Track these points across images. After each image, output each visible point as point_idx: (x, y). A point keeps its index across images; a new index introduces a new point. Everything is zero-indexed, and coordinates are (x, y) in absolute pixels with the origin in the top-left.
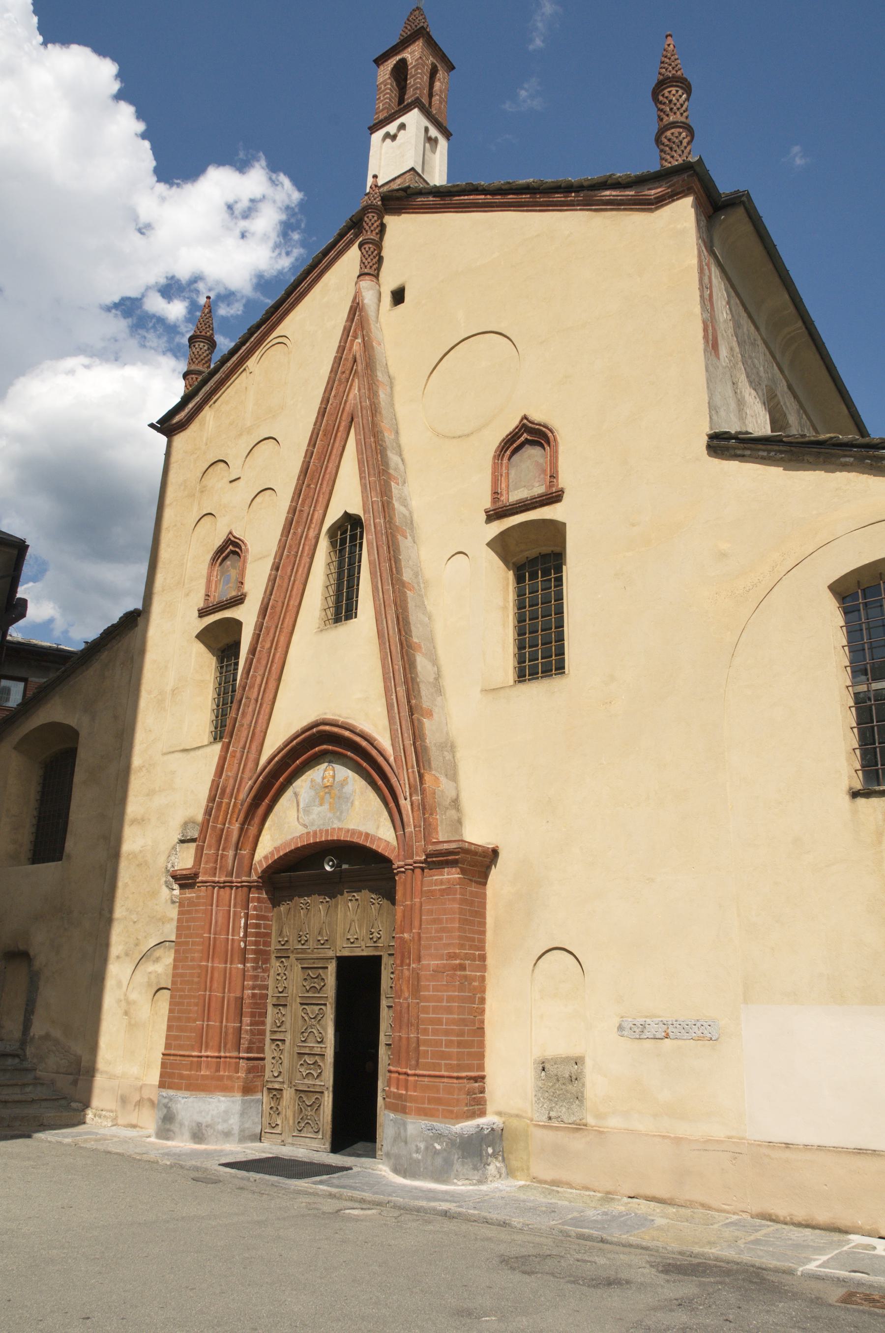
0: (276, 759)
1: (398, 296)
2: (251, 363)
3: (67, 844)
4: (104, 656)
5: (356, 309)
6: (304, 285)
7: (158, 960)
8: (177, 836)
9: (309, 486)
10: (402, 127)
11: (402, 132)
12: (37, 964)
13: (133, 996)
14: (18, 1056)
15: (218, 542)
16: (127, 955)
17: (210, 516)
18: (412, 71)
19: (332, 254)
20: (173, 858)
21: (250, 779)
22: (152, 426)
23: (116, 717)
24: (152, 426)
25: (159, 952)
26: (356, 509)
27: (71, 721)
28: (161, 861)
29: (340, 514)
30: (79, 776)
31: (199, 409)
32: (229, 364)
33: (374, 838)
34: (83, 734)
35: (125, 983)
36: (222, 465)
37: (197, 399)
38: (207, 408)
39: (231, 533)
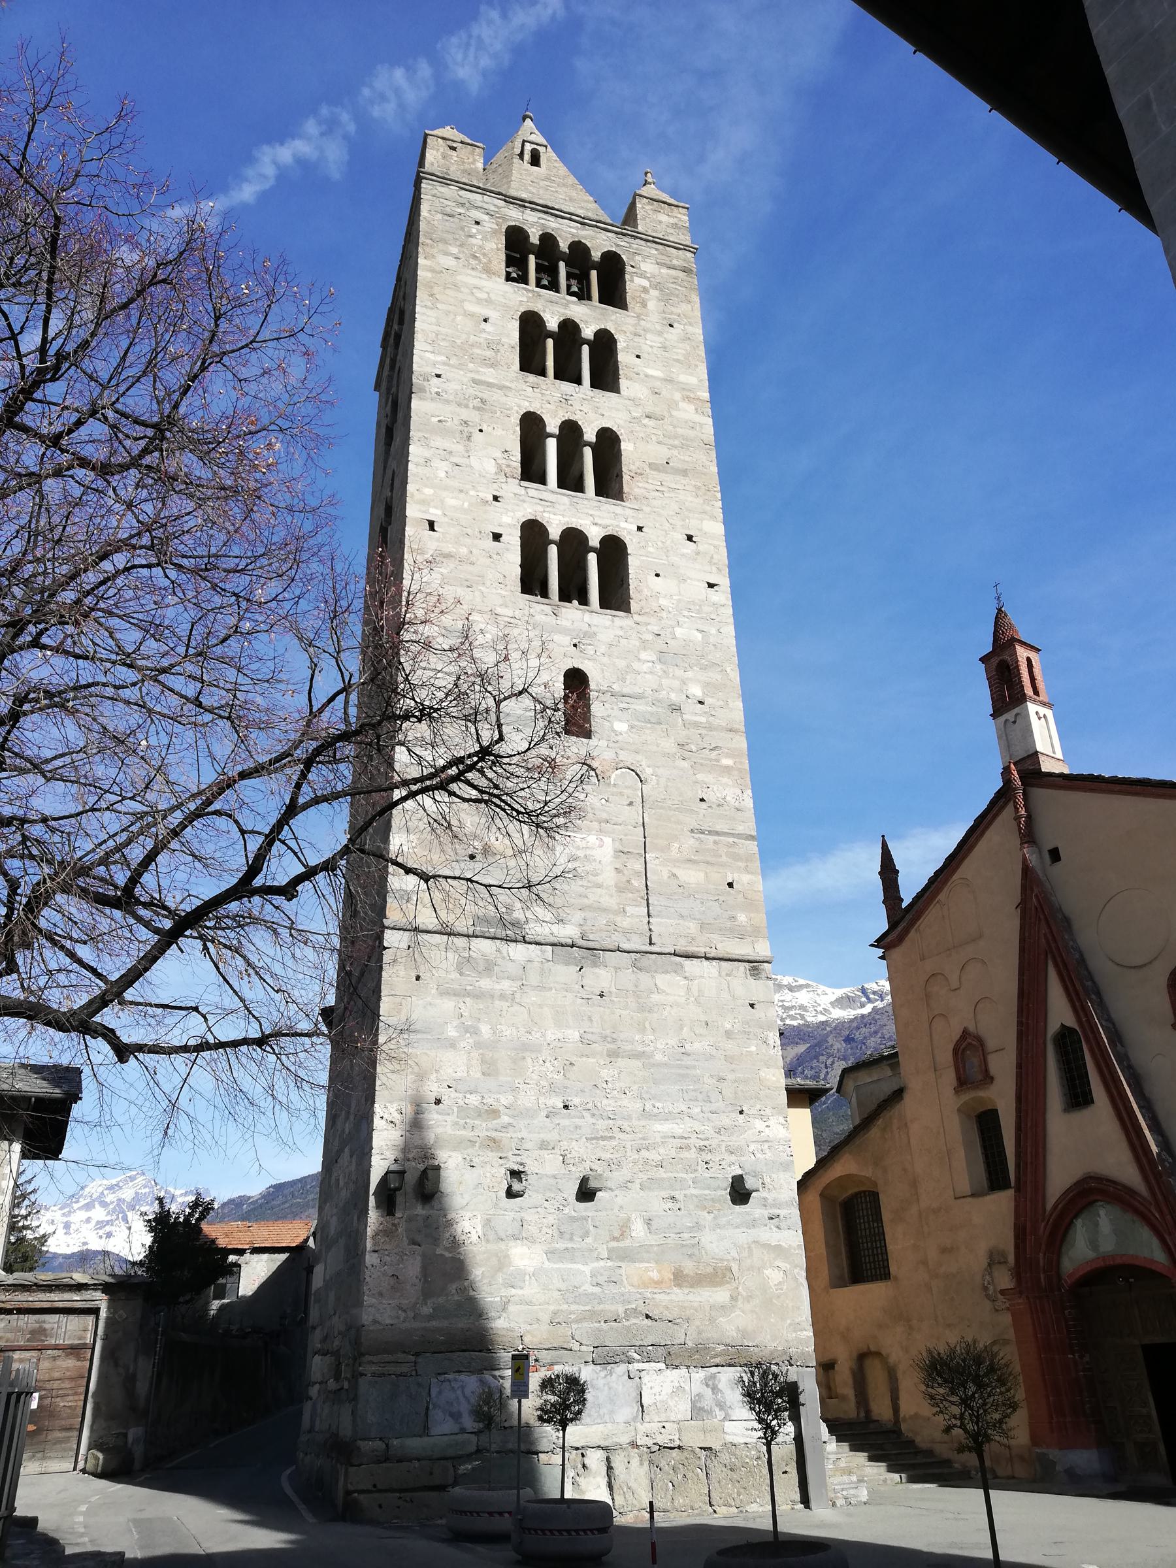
0: (1060, 1206)
1: (1055, 855)
2: (942, 896)
5: (1026, 870)
6: (972, 840)
8: (984, 1262)
9: (1028, 1005)
14: (894, 1432)
21: (1043, 1221)
22: (872, 945)
23: (905, 1170)
26: (1070, 1021)
27: (868, 1172)
29: (1059, 1026)
31: (906, 931)
33: (1152, 1261)
36: (939, 976)
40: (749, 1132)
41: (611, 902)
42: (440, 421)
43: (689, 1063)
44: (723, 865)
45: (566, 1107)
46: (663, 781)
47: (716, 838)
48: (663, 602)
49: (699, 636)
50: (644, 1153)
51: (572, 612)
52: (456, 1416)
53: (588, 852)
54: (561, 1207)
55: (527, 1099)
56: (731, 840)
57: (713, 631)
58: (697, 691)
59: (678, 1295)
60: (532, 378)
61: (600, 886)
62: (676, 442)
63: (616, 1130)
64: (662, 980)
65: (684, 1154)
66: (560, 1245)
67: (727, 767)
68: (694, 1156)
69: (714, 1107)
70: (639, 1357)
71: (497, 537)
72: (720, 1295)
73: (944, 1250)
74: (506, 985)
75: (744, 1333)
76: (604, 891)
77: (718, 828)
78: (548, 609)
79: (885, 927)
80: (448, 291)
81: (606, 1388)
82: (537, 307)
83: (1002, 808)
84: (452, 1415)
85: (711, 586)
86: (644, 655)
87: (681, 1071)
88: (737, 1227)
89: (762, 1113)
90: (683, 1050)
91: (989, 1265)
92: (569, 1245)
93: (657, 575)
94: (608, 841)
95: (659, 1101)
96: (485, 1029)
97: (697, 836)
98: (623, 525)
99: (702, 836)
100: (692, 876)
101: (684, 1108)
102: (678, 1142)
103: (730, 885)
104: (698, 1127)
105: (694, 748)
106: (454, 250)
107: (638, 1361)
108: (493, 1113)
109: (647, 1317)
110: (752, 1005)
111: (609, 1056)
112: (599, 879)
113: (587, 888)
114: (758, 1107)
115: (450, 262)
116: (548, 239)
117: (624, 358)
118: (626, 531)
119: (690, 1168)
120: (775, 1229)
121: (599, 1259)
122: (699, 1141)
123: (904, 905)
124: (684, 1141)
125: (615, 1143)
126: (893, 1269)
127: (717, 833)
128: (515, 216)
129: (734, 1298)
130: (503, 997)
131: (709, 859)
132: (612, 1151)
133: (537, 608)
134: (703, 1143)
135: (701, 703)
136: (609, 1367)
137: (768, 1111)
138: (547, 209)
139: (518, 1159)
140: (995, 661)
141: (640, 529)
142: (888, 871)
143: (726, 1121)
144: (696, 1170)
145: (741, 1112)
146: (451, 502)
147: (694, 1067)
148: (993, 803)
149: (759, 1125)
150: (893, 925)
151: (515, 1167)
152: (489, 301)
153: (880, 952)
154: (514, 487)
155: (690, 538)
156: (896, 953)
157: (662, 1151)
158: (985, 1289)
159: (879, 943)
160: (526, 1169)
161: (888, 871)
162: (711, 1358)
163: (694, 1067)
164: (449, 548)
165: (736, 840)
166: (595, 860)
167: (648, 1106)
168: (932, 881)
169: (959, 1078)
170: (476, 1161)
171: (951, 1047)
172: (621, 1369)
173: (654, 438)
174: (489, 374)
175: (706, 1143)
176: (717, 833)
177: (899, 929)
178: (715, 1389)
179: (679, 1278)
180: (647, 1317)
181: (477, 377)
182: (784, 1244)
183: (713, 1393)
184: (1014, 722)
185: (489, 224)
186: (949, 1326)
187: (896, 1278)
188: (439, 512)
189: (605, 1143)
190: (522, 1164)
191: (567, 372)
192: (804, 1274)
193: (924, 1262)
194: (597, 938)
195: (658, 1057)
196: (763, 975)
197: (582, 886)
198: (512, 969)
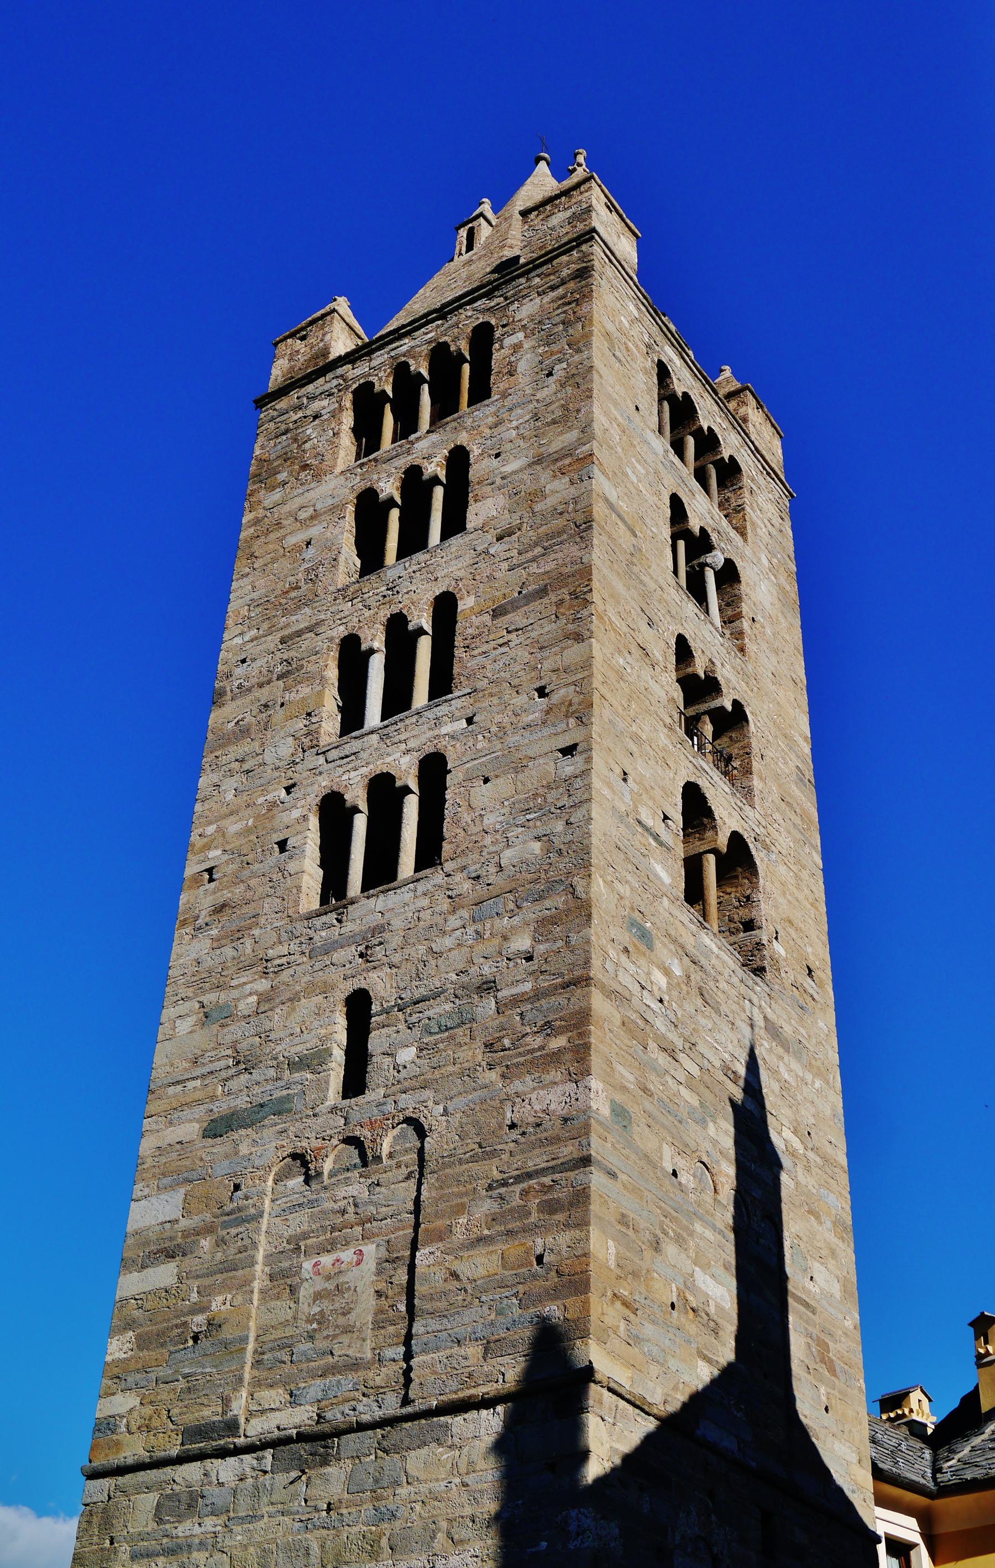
42: (237, 723)
53: (342, 1279)
56: (547, 1180)
57: (559, 826)
61: (348, 1330)
62: (538, 550)
64: (416, 1460)
74: (210, 1523)
77: (531, 1165)
93: (486, 781)
105: (507, 1042)
141: (470, 721)
188: (219, 852)
197: (327, 1337)
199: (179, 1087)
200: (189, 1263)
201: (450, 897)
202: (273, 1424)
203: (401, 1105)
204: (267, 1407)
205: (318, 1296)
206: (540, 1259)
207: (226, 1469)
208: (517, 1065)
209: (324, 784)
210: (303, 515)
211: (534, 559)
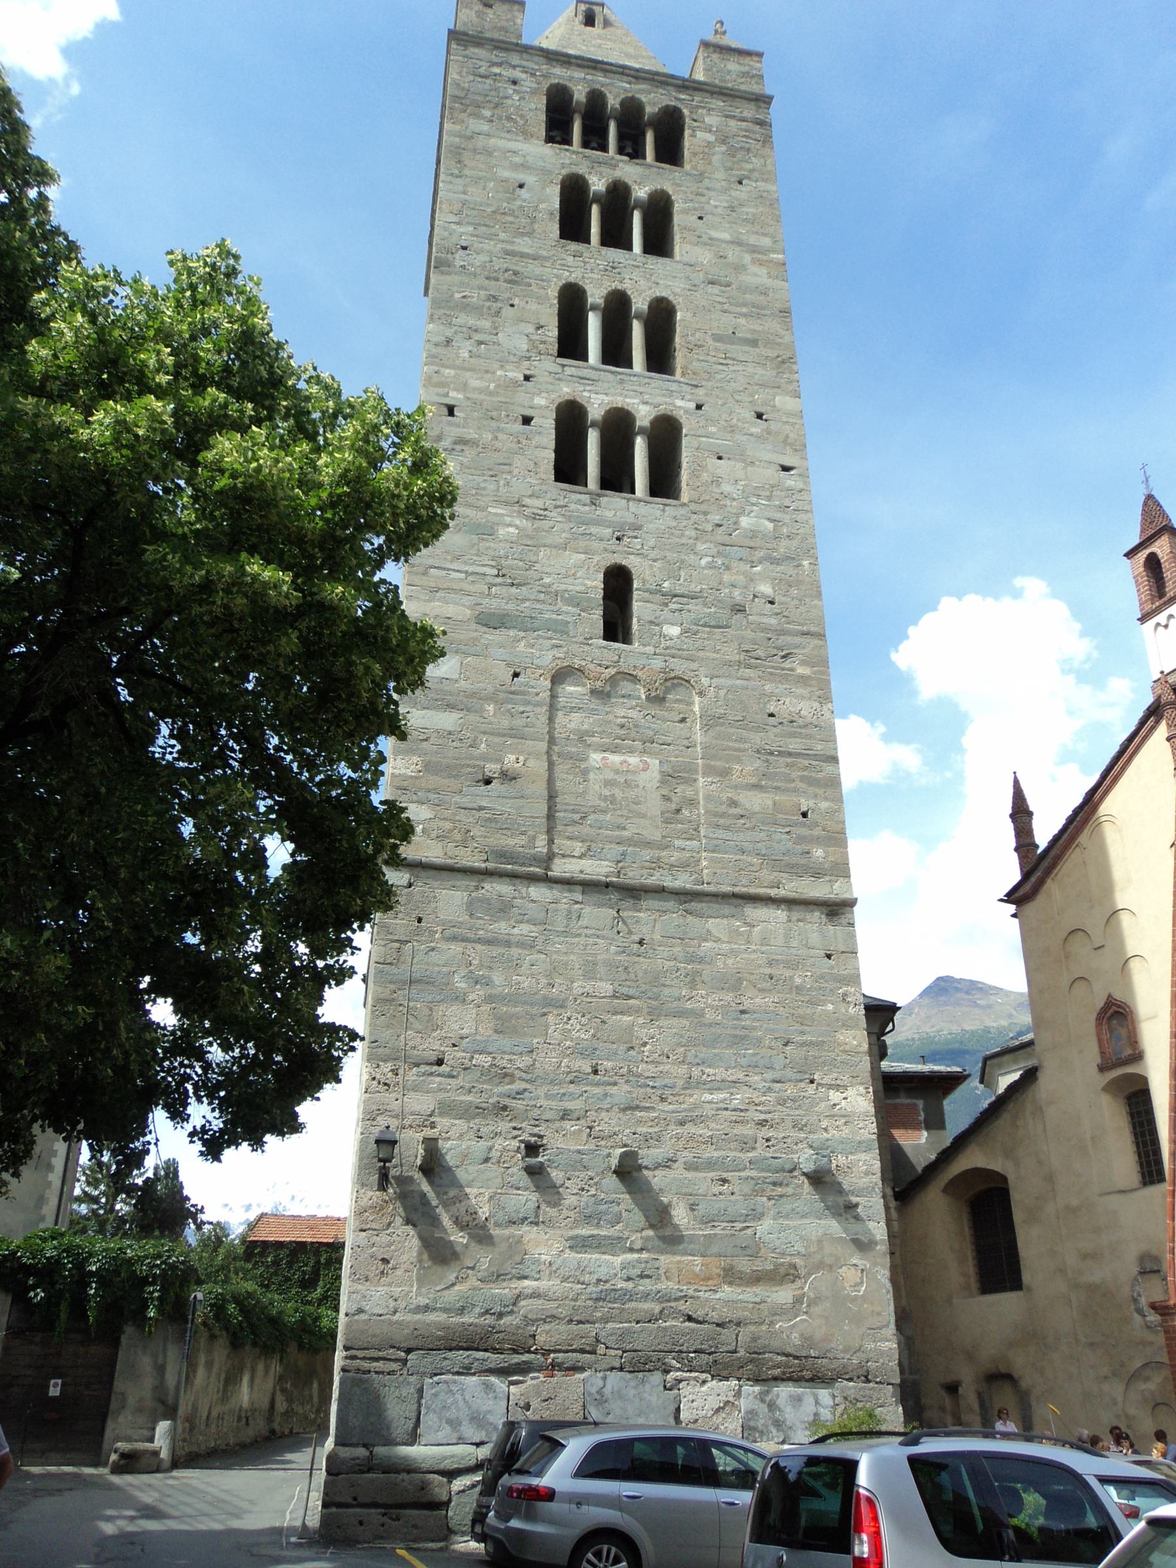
3: (1024, 1278)
4: (1011, 1106)
6: (1117, 768)
7: (1147, 1379)
8: (1135, 1270)
10: (1171, 616)
11: (1172, 620)
12: (1024, 1384)
13: (1132, 1411)
15: (1100, 1004)
16: (1114, 1375)
17: (1082, 983)
18: (1165, 565)
19: (1137, 740)
20: (1137, 1288)
22: (1001, 900)
23: (1040, 1163)
24: (1001, 900)
25: (1148, 1372)
28: (1126, 1291)
30: (1018, 1216)
31: (1041, 883)
32: (1061, 841)
34: (1011, 1179)
35: (1120, 1399)
36: (1080, 933)
37: (1038, 874)
38: (1049, 881)
39: (1110, 996)
40: (823, 1105)
41: (654, 834)
42: (464, 297)
43: (748, 1023)
44: (795, 790)
45: (595, 1072)
46: (722, 693)
47: (789, 760)
48: (727, 488)
49: (770, 526)
50: (690, 1129)
51: (614, 505)
52: (454, 1424)
54: (586, 1187)
55: (547, 1061)
56: (806, 763)
58: (766, 589)
59: (727, 1292)
60: (573, 246)
62: (744, 310)
63: (654, 1098)
64: (715, 925)
65: (740, 1130)
66: (585, 1231)
67: (802, 677)
68: (750, 1133)
69: (777, 1075)
70: (679, 1365)
71: (527, 420)
72: (783, 1295)
73: (1085, 1257)
74: (523, 930)
75: (807, 1339)
76: (647, 822)
78: (585, 498)
79: (1016, 877)
80: (478, 157)
81: (637, 1400)
82: (582, 170)
83: (1153, 728)
84: (450, 1422)
85: (786, 469)
86: (701, 547)
87: (738, 1032)
88: (802, 1217)
89: (838, 1082)
90: (741, 1007)
91: (1141, 1273)
92: (595, 1232)
93: (720, 458)
94: (654, 763)
95: (710, 1066)
96: (498, 978)
97: (764, 758)
98: (679, 403)
99: (771, 758)
100: (756, 802)
101: (741, 1075)
102: (733, 1116)
103: (805, 815)
104: (756, 1097)
106: (487, 113)
107: (679, 1370)
108: (506, 1076)
109: (690, 1319)
110: (829, 956)
111: (649, 1013)
112: (642, 808)
113: (628, 818)
114: (835, 1075)
115: (485, 127)
116: (596, 99)
117: (680, 218)
118: (681, 407)
119: (746, 1144)
120: (852, 1220)
121: (631, 1250)
122: (757, 1114)
123: (1039, 851)
124: (738, 1113)
125: (656, 1115)
126: (1026, 1277)
127: (790, 754)
128: (560, 74)
129: (798, 1300)
130: (521, 945)
131: (780, 784)
132: (650, 1124)
133: (573, 498)
134: (763, 1117)
135: (772, 603)
136: (640, 1375)
137: (846, 1079)
138: (594, 65)
139: (536, 1130)
140: (1142, 556)
142: (1021, 813)
143: (790, 1090)
144: (754, 1148)
145: (812, 1082)
146: (475, 383)
147: (755, 1028)
148: (1142, 723)
149: (835, 1096)
150: (1026, 876)
151: (533, 1139)
152: (524, 167)
153: (1012, 908)
154: (548, 365)
155: (759, 416)
156: (1031, 908)
157: (713, 1125)
158: (1135, 1300)
159: (1012, 897)
160: (545, 1142)
161: (1021, 813)
162: (769, 1369)
163: (755, 1028)
164: (471, 433)
165: (814, 763)
166: (637, 786)
167: (696, 1072)
168: (1070, 820)
169: (1102, 1053)
170: (484, 1131)
171: (1093, 1016)
172: (657, 1377)
173: (718, 307)
174: (524, 245)
175: (768, 1117)
176: (790, 754)
177: (1033, 879)
178: (772, 1406)
179: (731, 1276)
180: (690, 1319)
181: (509, 247)
182: (863, 1238)
183: (770, 1411)
184: (1166, 626)
185: (528, 83)
186: (1092, 1345)
187: (1029, 1289)
188: (460, 396)
189: (642, 1114)
190: (541, 1137)
191: (615, 237)
192: (887, 1273)
193: (1062, 1271)
194: (635, 876)
195: (710, 1016)
196: (844, 921)
198: (533, 911)
199: (444, 573)
200: (472, 717)
201: (696, 529)
202: (578, 868)
203: (672, 666)
204: (568, 852)
205: (607, 783)
206: (805, 815)
207: (537, 892)
208: (771, 674)
209: (566, 390)
210: (517, 159)
211: (745, 315)
